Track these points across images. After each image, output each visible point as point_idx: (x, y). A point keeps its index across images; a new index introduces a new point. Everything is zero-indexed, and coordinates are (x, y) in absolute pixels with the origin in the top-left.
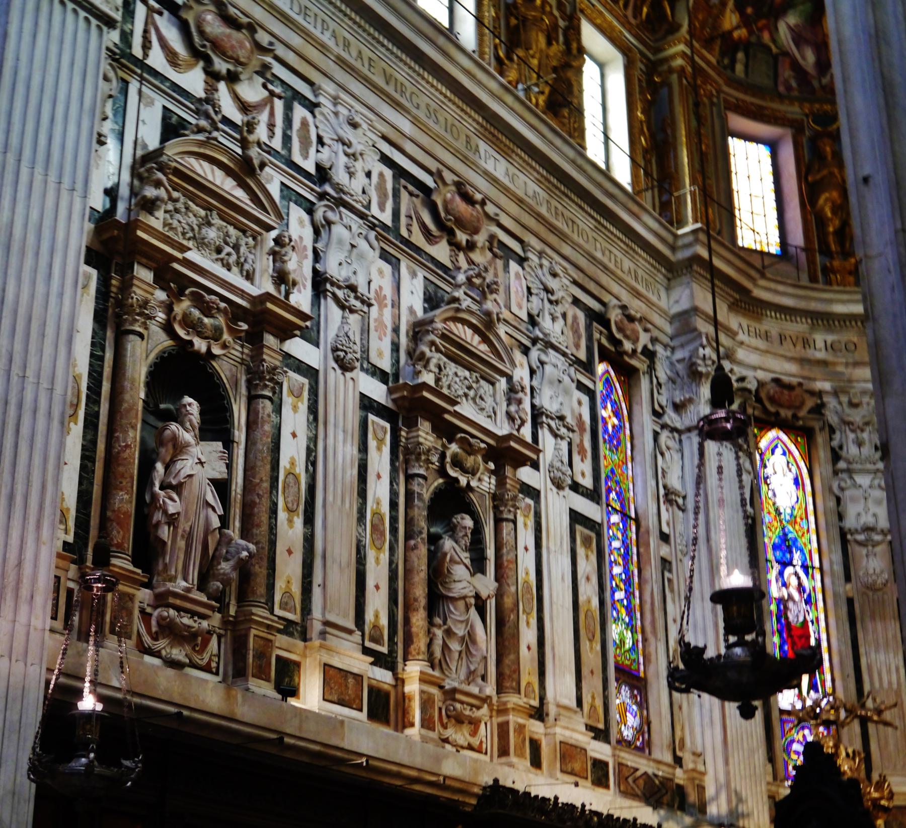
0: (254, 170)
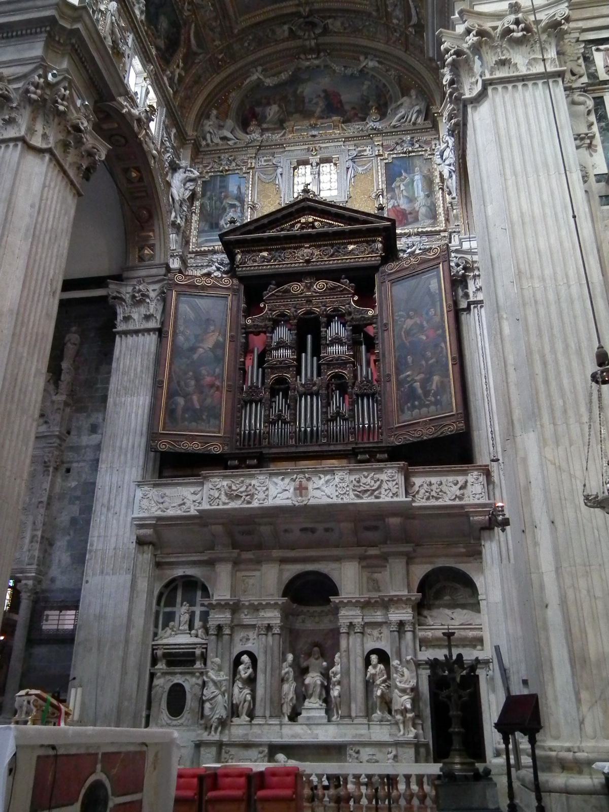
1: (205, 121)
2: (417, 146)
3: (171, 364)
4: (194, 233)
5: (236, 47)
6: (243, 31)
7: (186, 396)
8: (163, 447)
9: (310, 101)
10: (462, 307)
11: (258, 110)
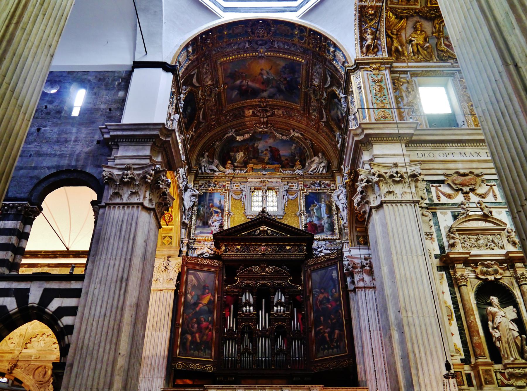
0: (488, 215)
1: (201, 158)
2: (323, 186)
3: (183, 313)
4: (193, 227)
5: (223, 118)
6: (227, 111)
7: (193, 334)
8: (179, 366)
9: (262, 152)
10: (349, 289)
11: (232, 154)
